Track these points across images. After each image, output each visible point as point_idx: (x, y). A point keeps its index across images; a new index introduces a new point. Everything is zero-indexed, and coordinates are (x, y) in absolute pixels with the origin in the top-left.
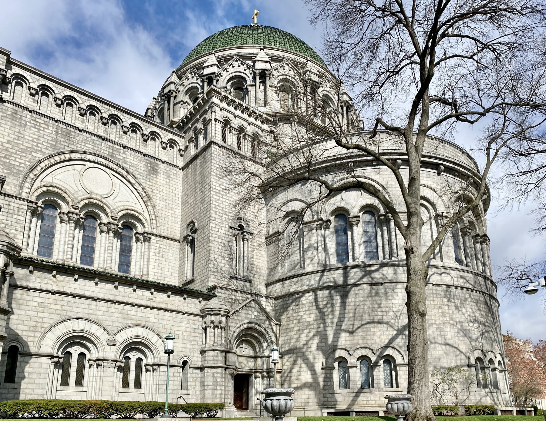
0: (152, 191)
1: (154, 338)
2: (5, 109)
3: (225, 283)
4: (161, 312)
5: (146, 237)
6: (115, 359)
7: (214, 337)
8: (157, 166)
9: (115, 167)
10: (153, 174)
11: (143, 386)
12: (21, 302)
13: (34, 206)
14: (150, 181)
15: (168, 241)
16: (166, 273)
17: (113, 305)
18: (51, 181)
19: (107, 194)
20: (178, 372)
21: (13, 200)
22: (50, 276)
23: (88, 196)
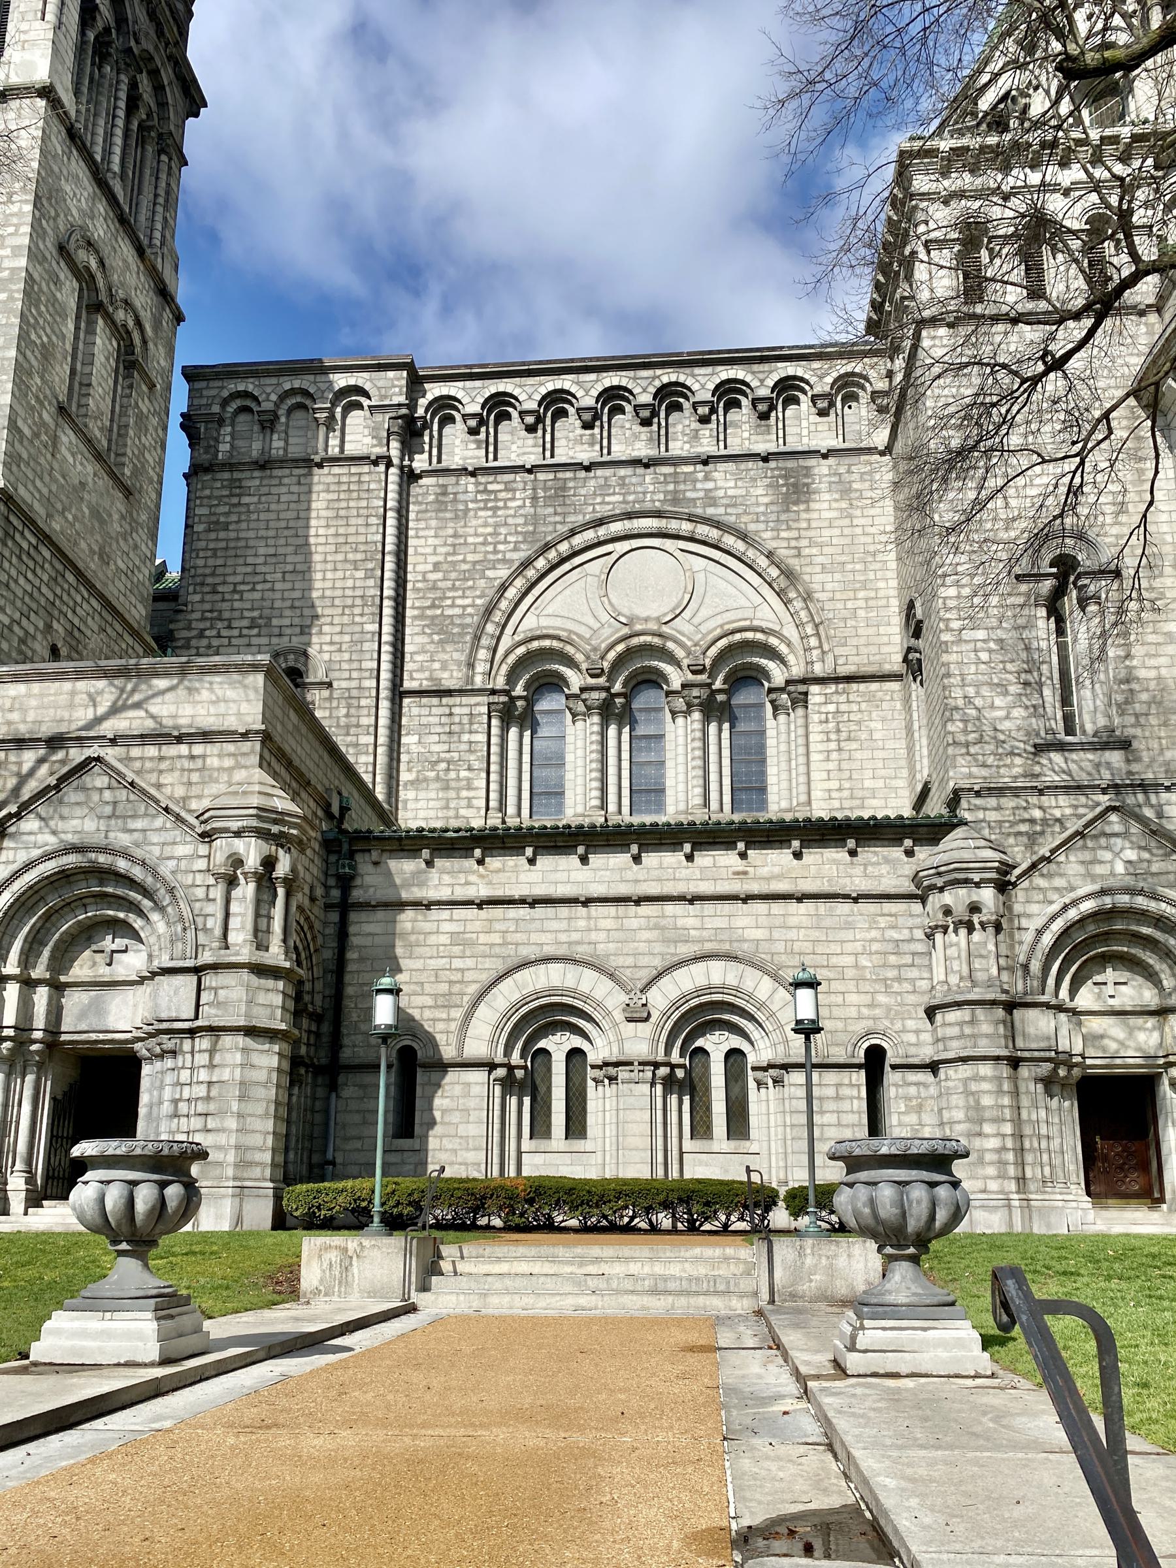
0: (799, 555)
3: (1017, 771)
5: (796, 694)
7: (955, 962)
9: (686, 527)
11: (753, 1133)
14: (789, 528)
15: (862, 687)
17: (632, 909)
18: (534, 625)
19: (673, 610)
20: (851, 1085)
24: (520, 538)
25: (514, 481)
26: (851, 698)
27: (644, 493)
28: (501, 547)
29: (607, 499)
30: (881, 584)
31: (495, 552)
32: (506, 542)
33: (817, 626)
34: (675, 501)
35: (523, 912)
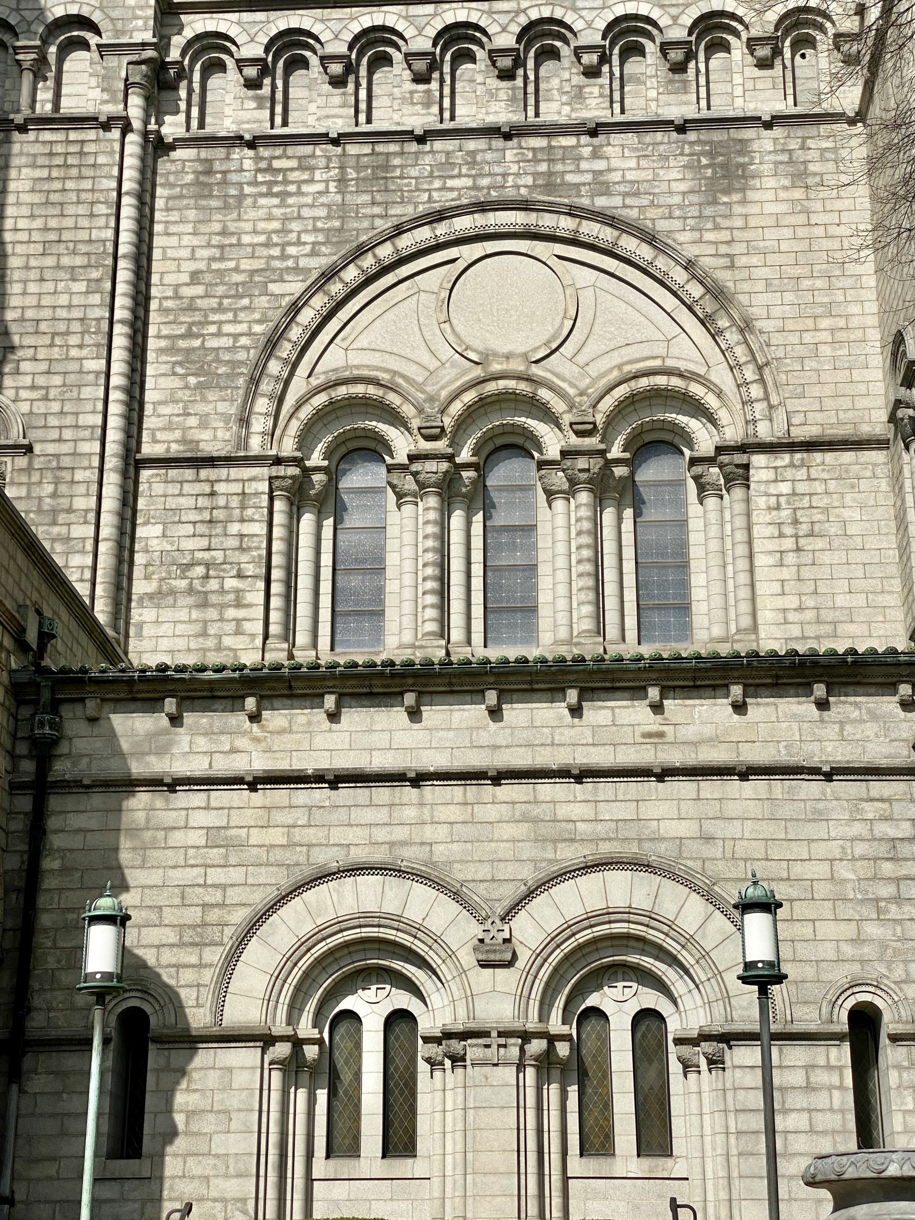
0: (732, 266)
1: (687, 912)
2: (176, 173)
4: (710, 788)
8: (741, 153)
9: (566, 224)
10: (727, 191)
12: (147, 835)
13: (293, 471)
14: (717, 228)
16: (841, 600)
21: (223, 472)
22: (239, 720)
23: (478, 372)
24: (321, 238)
25: (313, 156)
26: (814, 473)
27: (504, 175)
28: (292, 250)
29: (450, 183)
30: (854, 309)
31: (284, 257)
32: (299, 243)
33: (760, 368)
34: (550, 187)
35: (320, 795)
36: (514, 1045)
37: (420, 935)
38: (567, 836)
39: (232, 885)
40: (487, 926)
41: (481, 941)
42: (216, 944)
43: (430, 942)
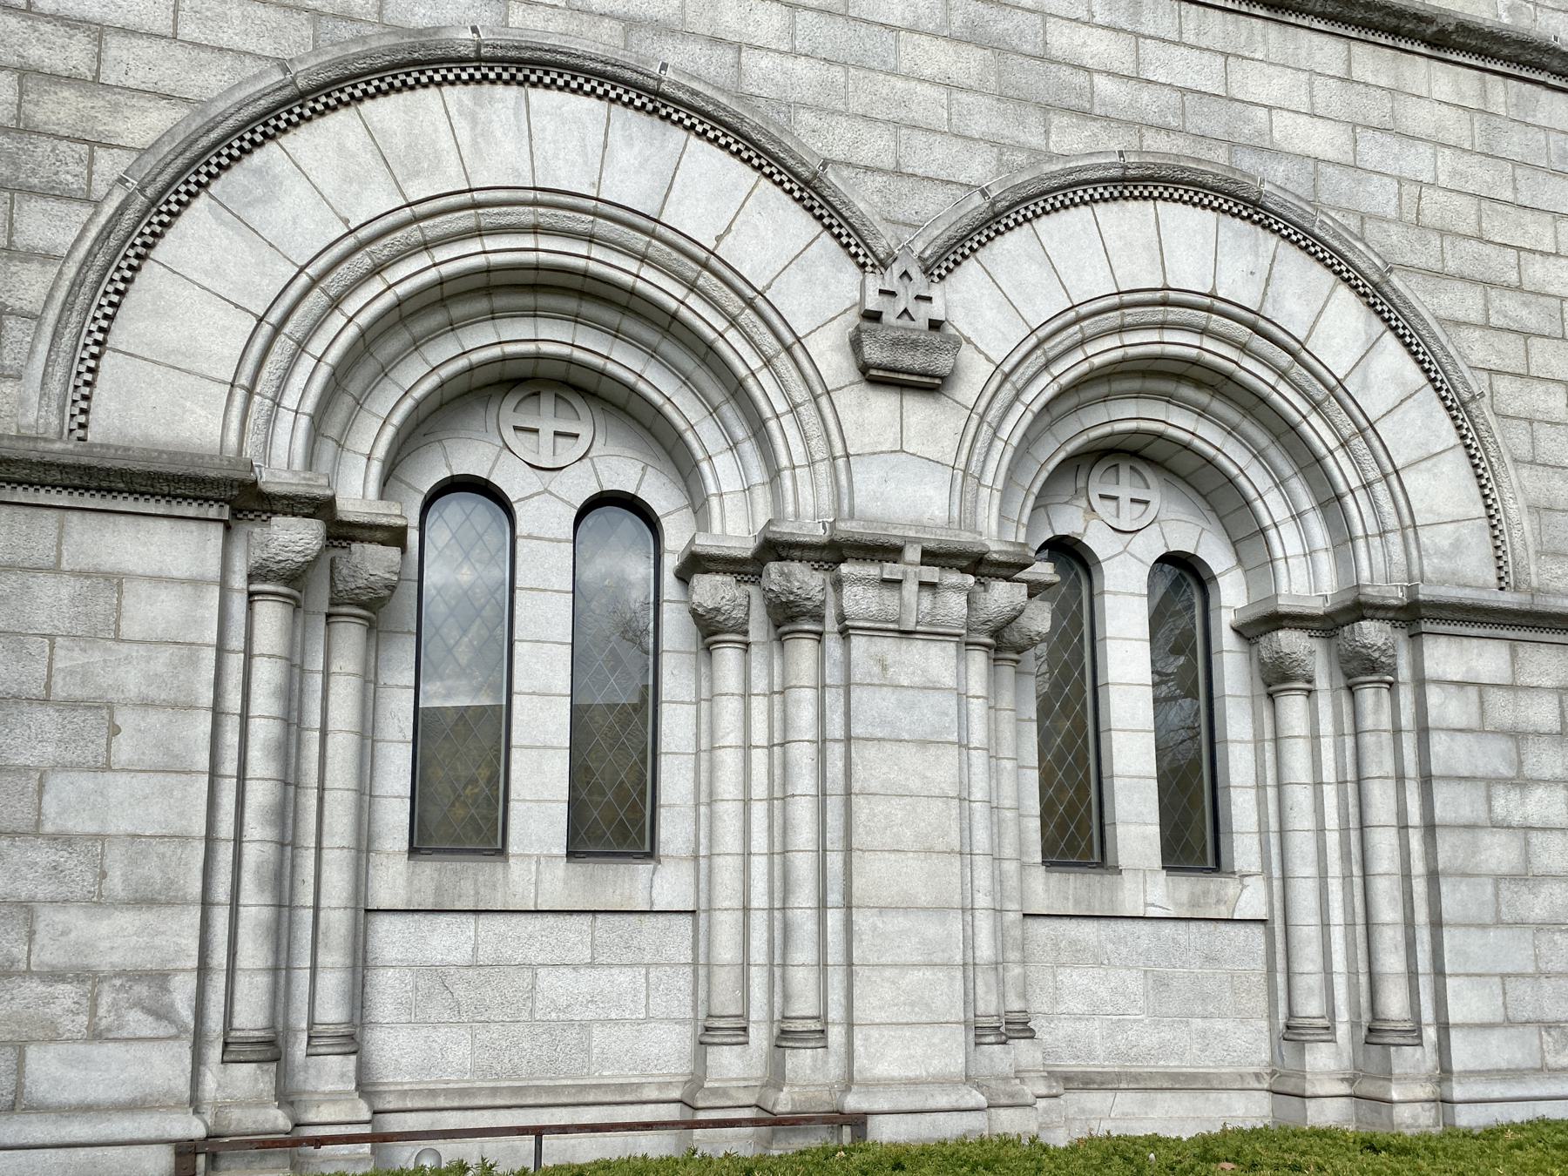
6: (963, 539)
36: (956, 588)
37: (706, 280)
38: (1074, 102)
39: (127, 32)
40: (891, 280)
41: (874, 317)
42: (67, 197)
43: (734, 304)
